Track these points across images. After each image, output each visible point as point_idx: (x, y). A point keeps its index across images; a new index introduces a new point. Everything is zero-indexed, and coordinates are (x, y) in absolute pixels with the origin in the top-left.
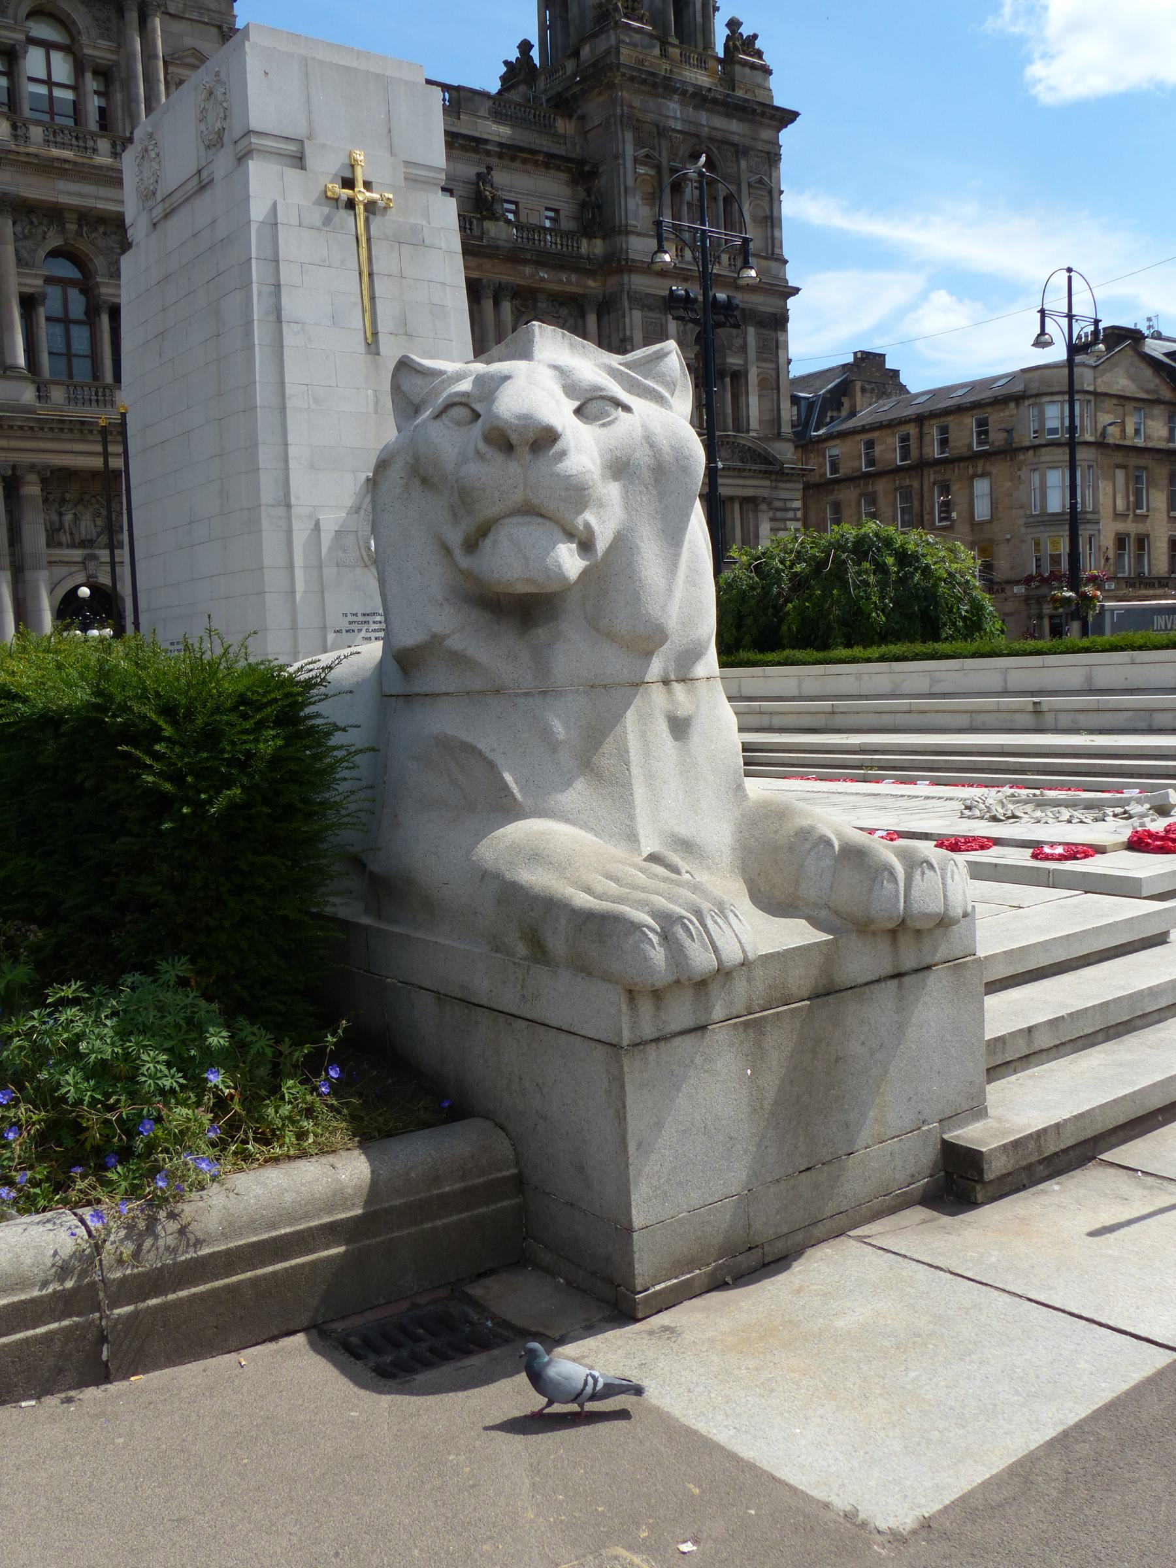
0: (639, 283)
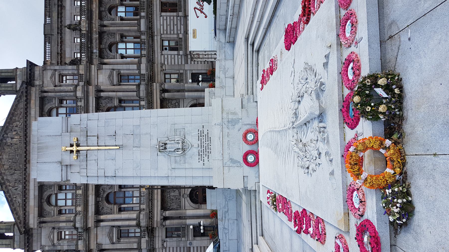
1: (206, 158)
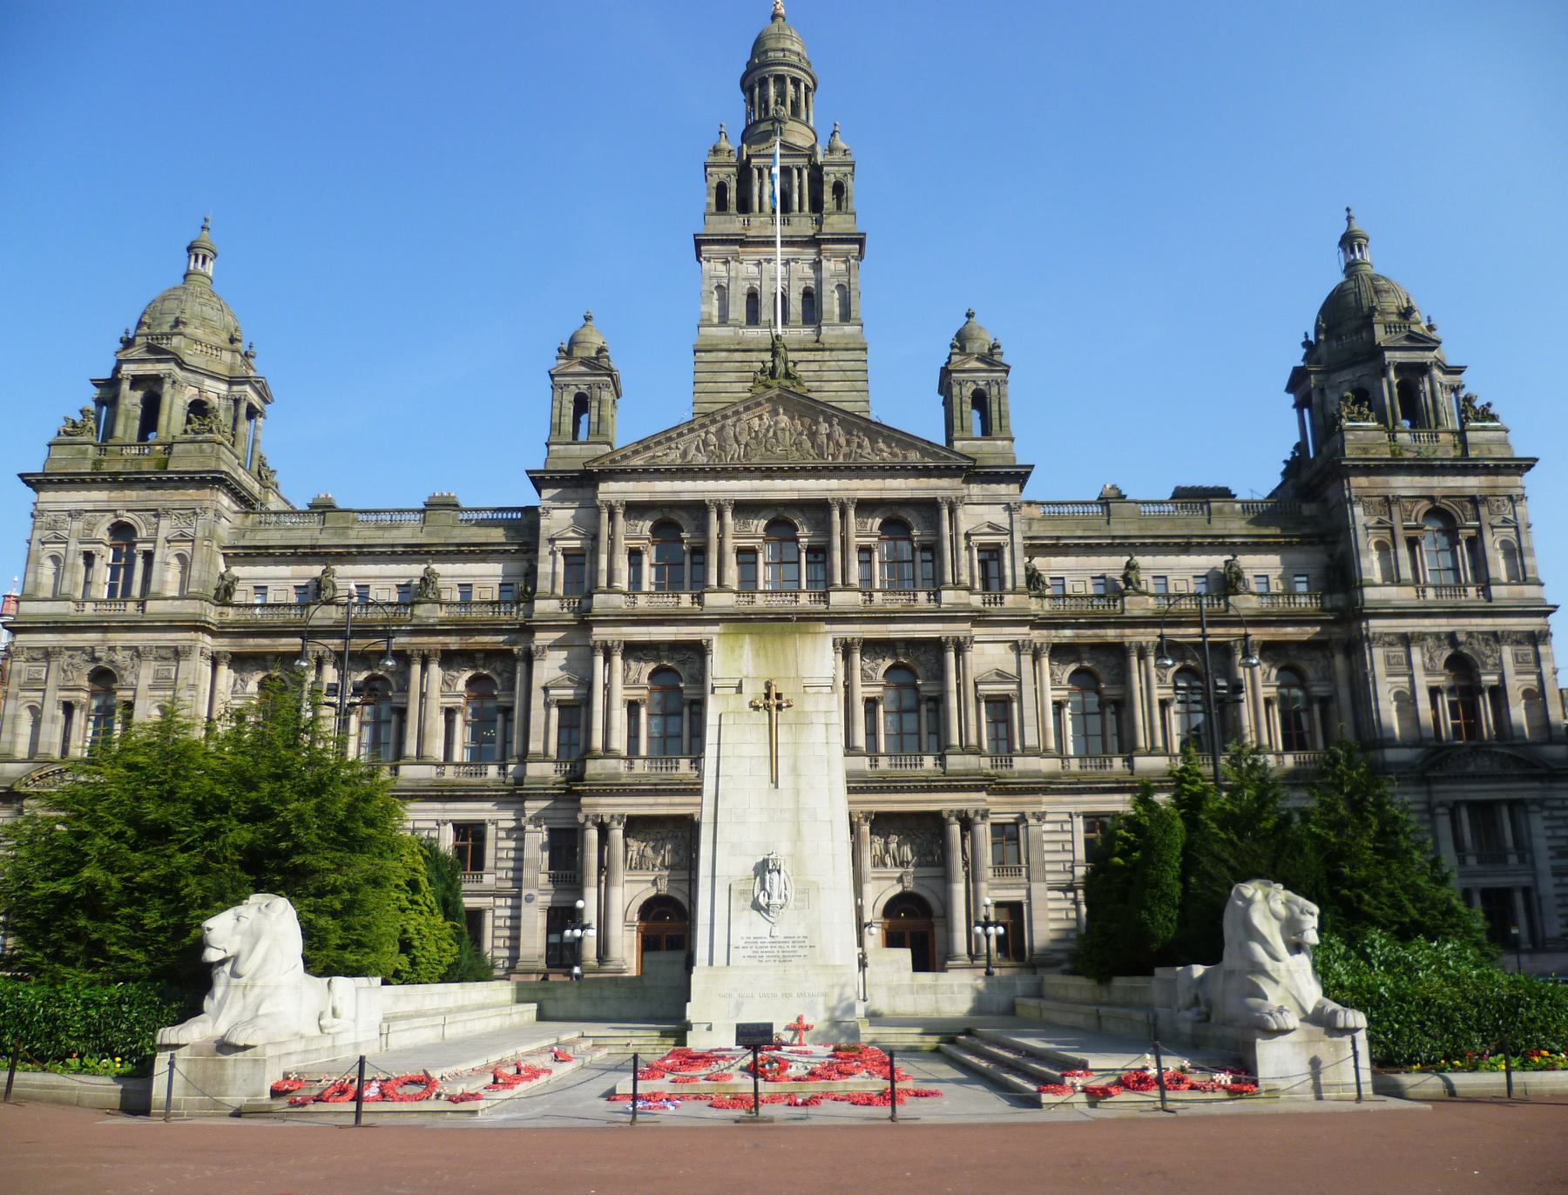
0: (1376, 626)
1: (749, 952)
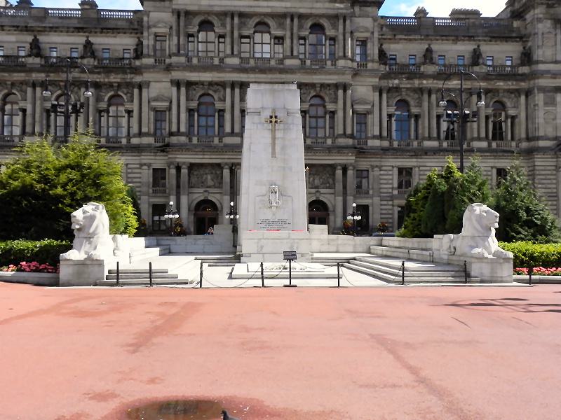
0: (542, 82)
